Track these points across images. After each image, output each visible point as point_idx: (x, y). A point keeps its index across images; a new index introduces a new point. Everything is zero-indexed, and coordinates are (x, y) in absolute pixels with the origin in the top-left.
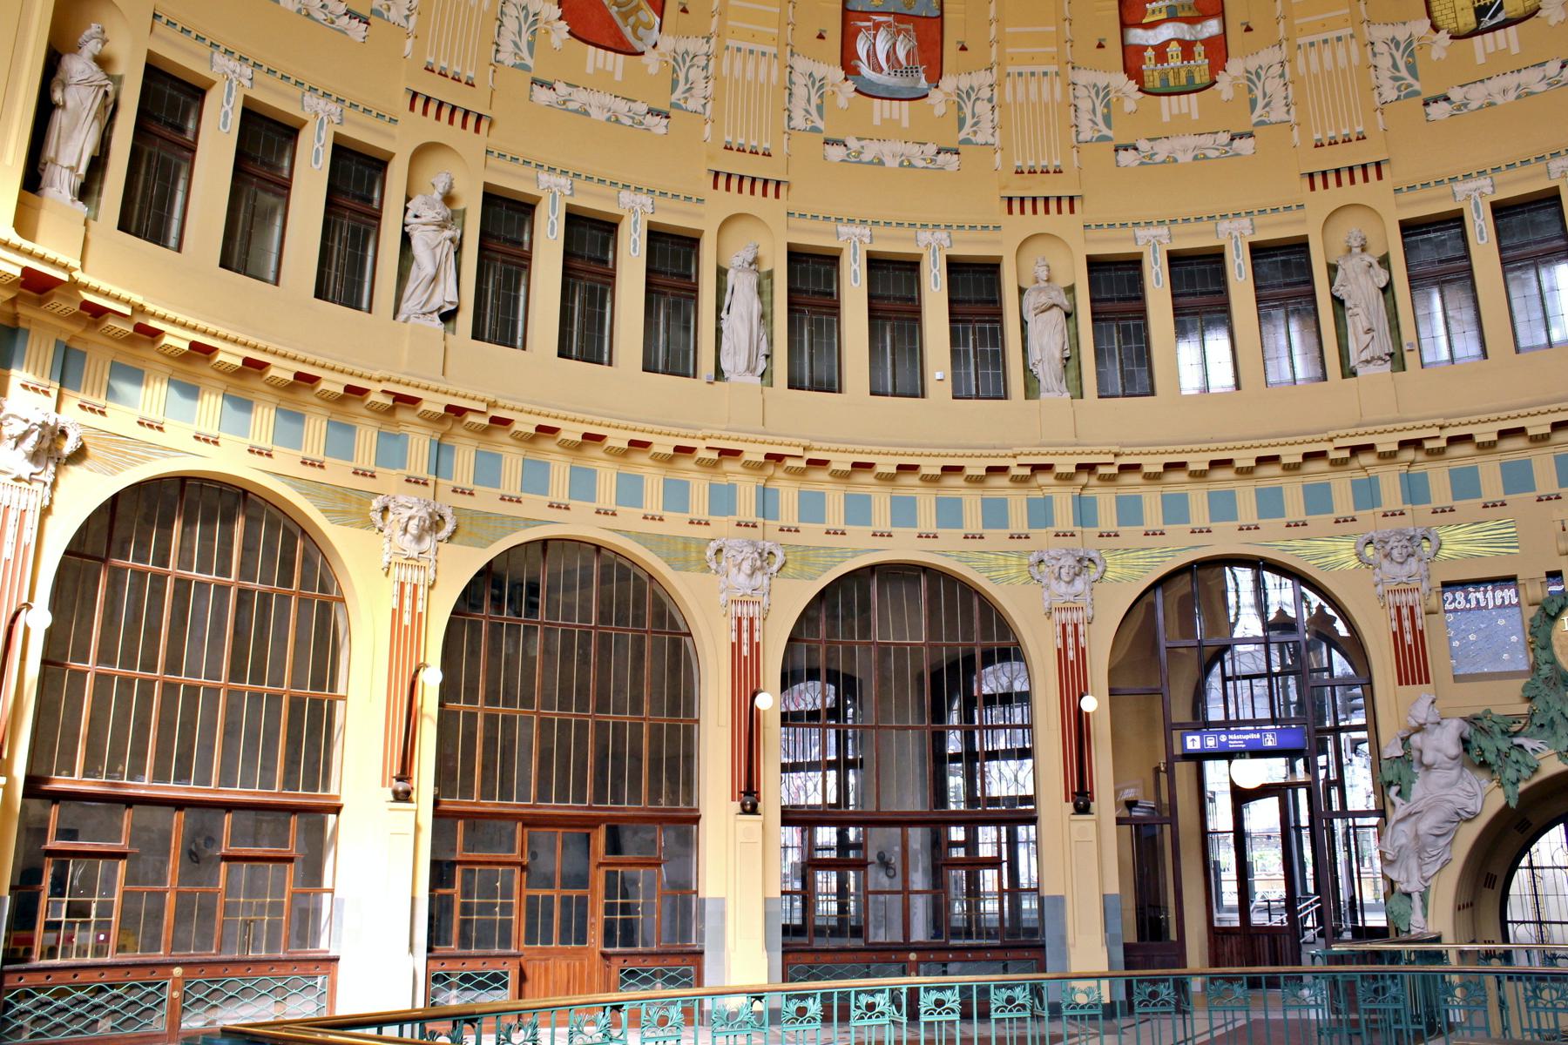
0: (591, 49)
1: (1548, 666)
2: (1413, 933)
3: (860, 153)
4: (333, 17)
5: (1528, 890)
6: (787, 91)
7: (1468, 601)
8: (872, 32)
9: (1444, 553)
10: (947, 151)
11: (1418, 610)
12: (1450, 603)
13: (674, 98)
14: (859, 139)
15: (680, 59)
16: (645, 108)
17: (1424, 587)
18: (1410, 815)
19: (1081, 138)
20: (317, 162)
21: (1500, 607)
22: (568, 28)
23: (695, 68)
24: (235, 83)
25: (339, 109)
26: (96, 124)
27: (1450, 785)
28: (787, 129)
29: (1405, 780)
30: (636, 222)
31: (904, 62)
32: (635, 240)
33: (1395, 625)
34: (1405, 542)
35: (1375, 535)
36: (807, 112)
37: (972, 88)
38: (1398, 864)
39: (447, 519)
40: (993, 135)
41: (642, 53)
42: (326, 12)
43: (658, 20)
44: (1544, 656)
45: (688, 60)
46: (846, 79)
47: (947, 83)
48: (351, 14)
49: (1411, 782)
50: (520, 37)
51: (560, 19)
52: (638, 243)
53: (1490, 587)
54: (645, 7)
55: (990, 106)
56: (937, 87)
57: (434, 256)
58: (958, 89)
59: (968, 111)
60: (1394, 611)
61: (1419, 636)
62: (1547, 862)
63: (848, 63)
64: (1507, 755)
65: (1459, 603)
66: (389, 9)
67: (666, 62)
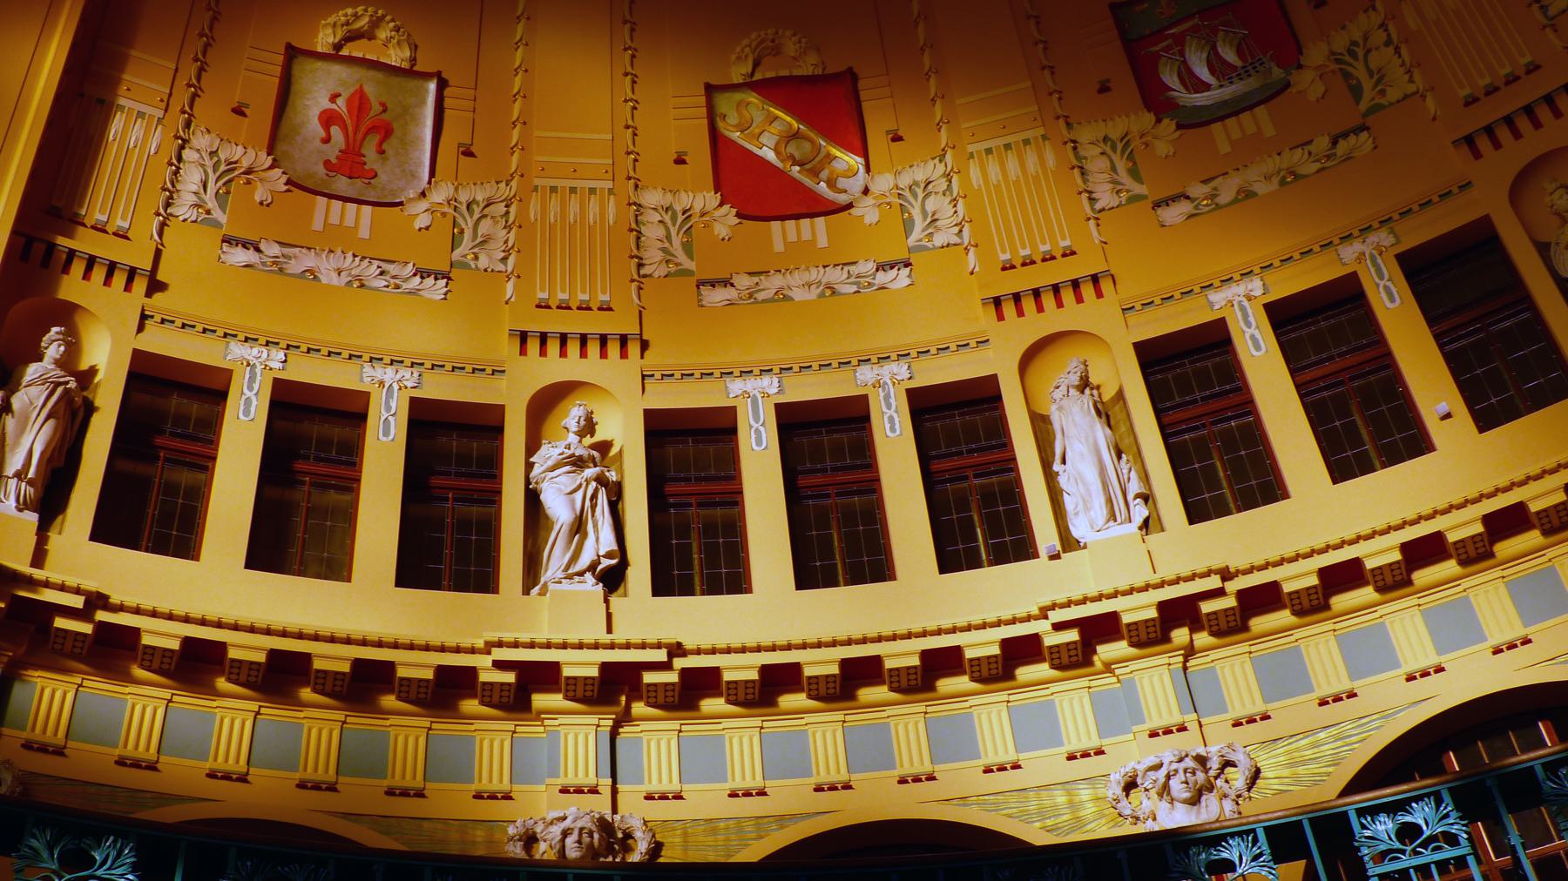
0: (776, 225)
3: (1216, 196)
4: (397, 281)
6: (1076, 171)
8: (1176, 50)
10: (1345, 135)
13: (912, 241)
14: (1205, 182)
15: (907, 193)
16: (871, 266)
19: (1552, 11)
20: (386, 434)
22: (734, 211)
23: (933, 196)
24: (259, 368)
25: (416, 375)
26: (51, 423)
28: (1090, 213)
30: (887, 397)
31: (1239, 63)
32: (891, 419)
36: (1114, 182)
37: (1354, 43)
39: (638, 834)
40: (1411, 81)
41: (850, 206)
42: (387, 278)
43: (861, 160)
45: (920, 191)
46: (1159, 121)
47: (1315, 55)
48: (423, 273)
50: (670, 242)
51: (721, 205)
52: (897, 420)
54: (838, 154)
55: (1391, 50)
56: (1300, 67)
57: (573, 502)
58: (1333, 53)
59: (1360, 72)
63: (1157, 102)
66: (476, 258)
67: (888, 204)
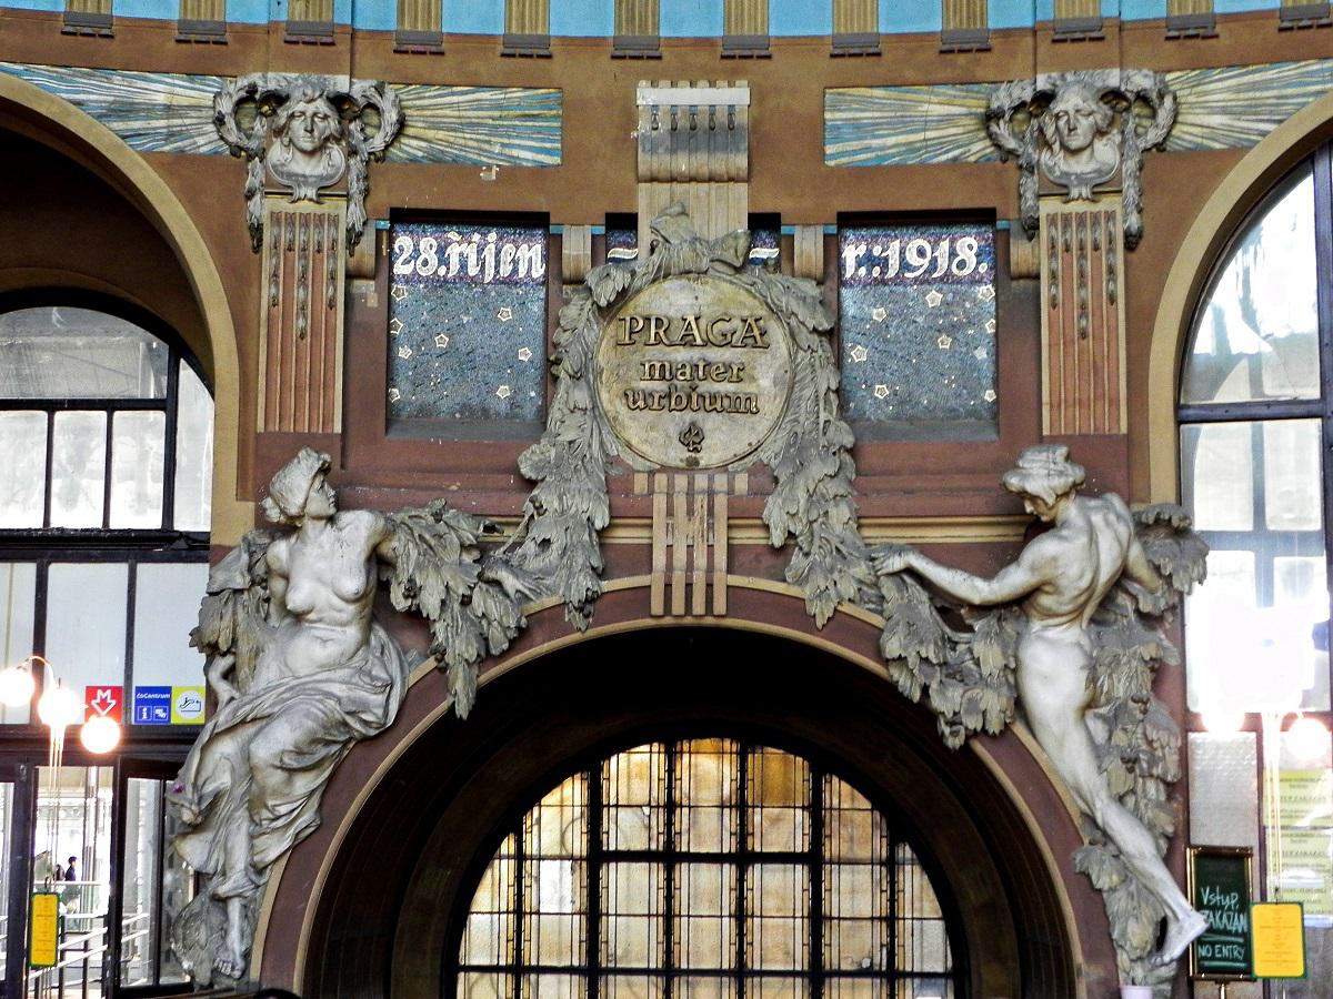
2: (216, 987)
5: (506, 899)
7: (444, 260)
9: (411, 147)
12: (407, 262)
18: (243, 722)
21: (504, 282)
34: (322, 106)
35: (260, 83)
38: (208, 836)
49: (257, 652)
62: (549, 843)
65: (425, 263)
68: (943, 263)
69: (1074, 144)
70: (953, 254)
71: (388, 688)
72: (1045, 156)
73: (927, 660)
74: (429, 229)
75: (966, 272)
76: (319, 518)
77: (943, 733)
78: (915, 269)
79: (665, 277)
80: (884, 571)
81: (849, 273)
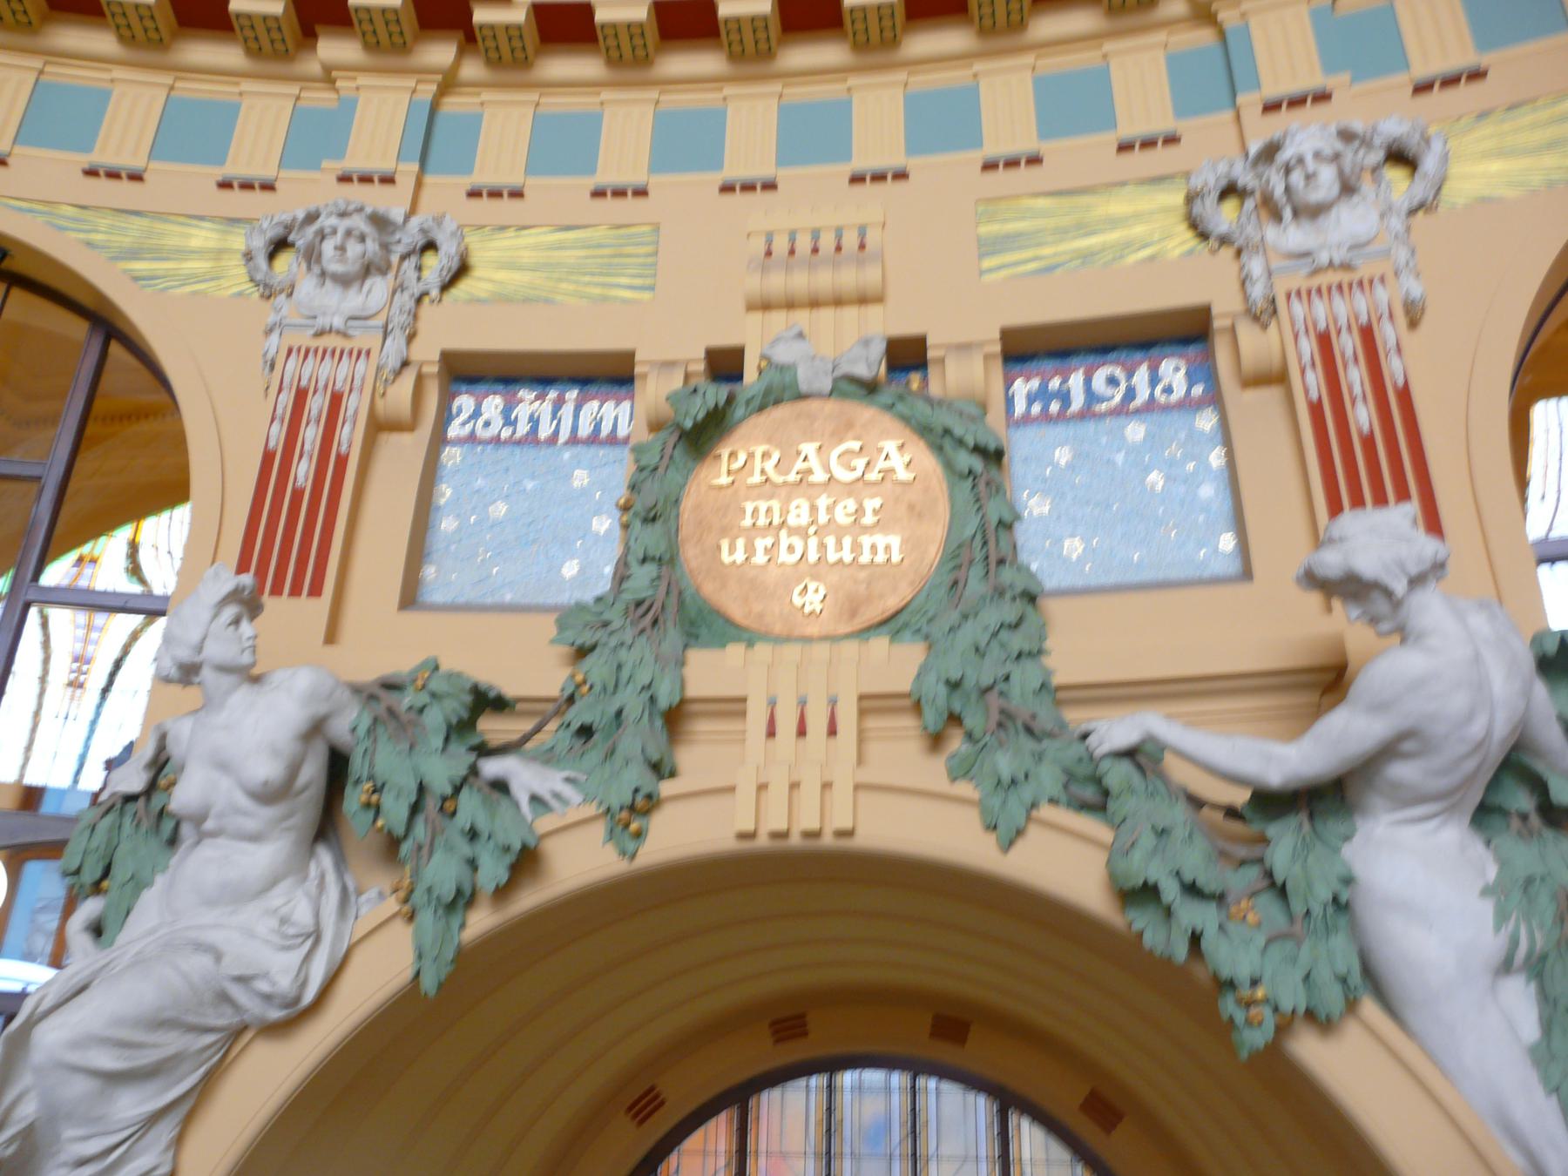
1: (651, 569)
7: (509, 422)
11: (356, 406)
17: (394, 348)
27: (238, 895)
29: (120, 873)
33: (278, 433)
34: (359, 223)
44: (650, 539)
49: (138, 884)
53: (572, 394)
60: (287, 399)
61: (330, 463)
64: (448, 808)
65: (487, 424)
68: (1143, 395)
69: (1317, 195)
70: (1154, 380)
71: (309, 943)
72: (1271, 232)
73: (1192, 890)
74: (501, 387)
75: (1179, 391)
76: (224, 669)
77: (1231, 1020)
78: (1101, 400)
79: (777, 402)
80: (1105, 748)
81: (1020, 407)
